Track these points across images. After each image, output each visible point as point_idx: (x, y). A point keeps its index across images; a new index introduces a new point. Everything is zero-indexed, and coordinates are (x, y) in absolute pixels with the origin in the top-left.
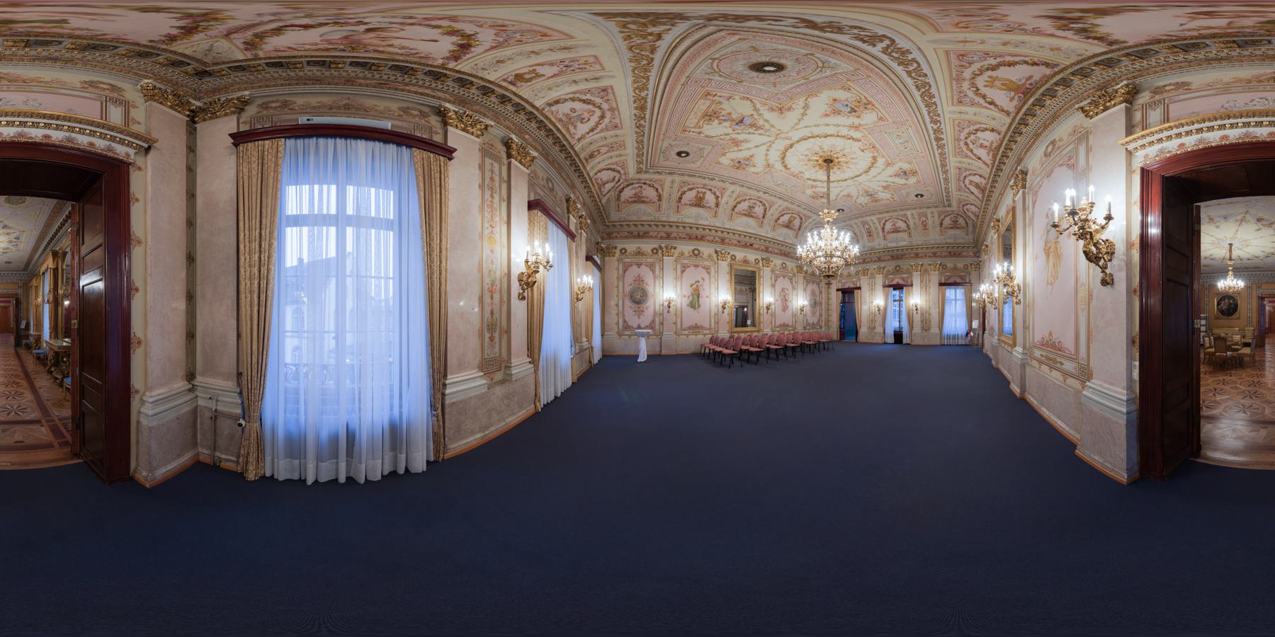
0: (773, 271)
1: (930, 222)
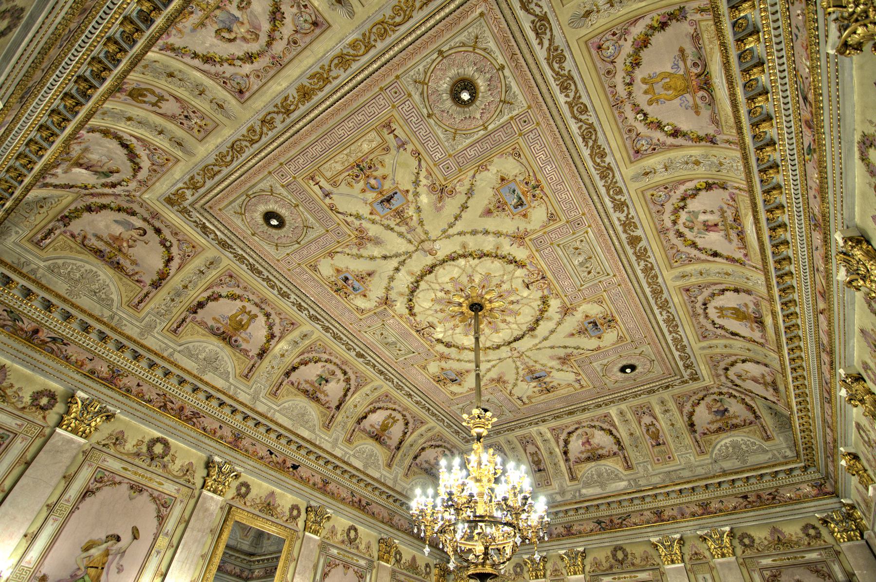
0: (324, 547)
1: (663, 424)
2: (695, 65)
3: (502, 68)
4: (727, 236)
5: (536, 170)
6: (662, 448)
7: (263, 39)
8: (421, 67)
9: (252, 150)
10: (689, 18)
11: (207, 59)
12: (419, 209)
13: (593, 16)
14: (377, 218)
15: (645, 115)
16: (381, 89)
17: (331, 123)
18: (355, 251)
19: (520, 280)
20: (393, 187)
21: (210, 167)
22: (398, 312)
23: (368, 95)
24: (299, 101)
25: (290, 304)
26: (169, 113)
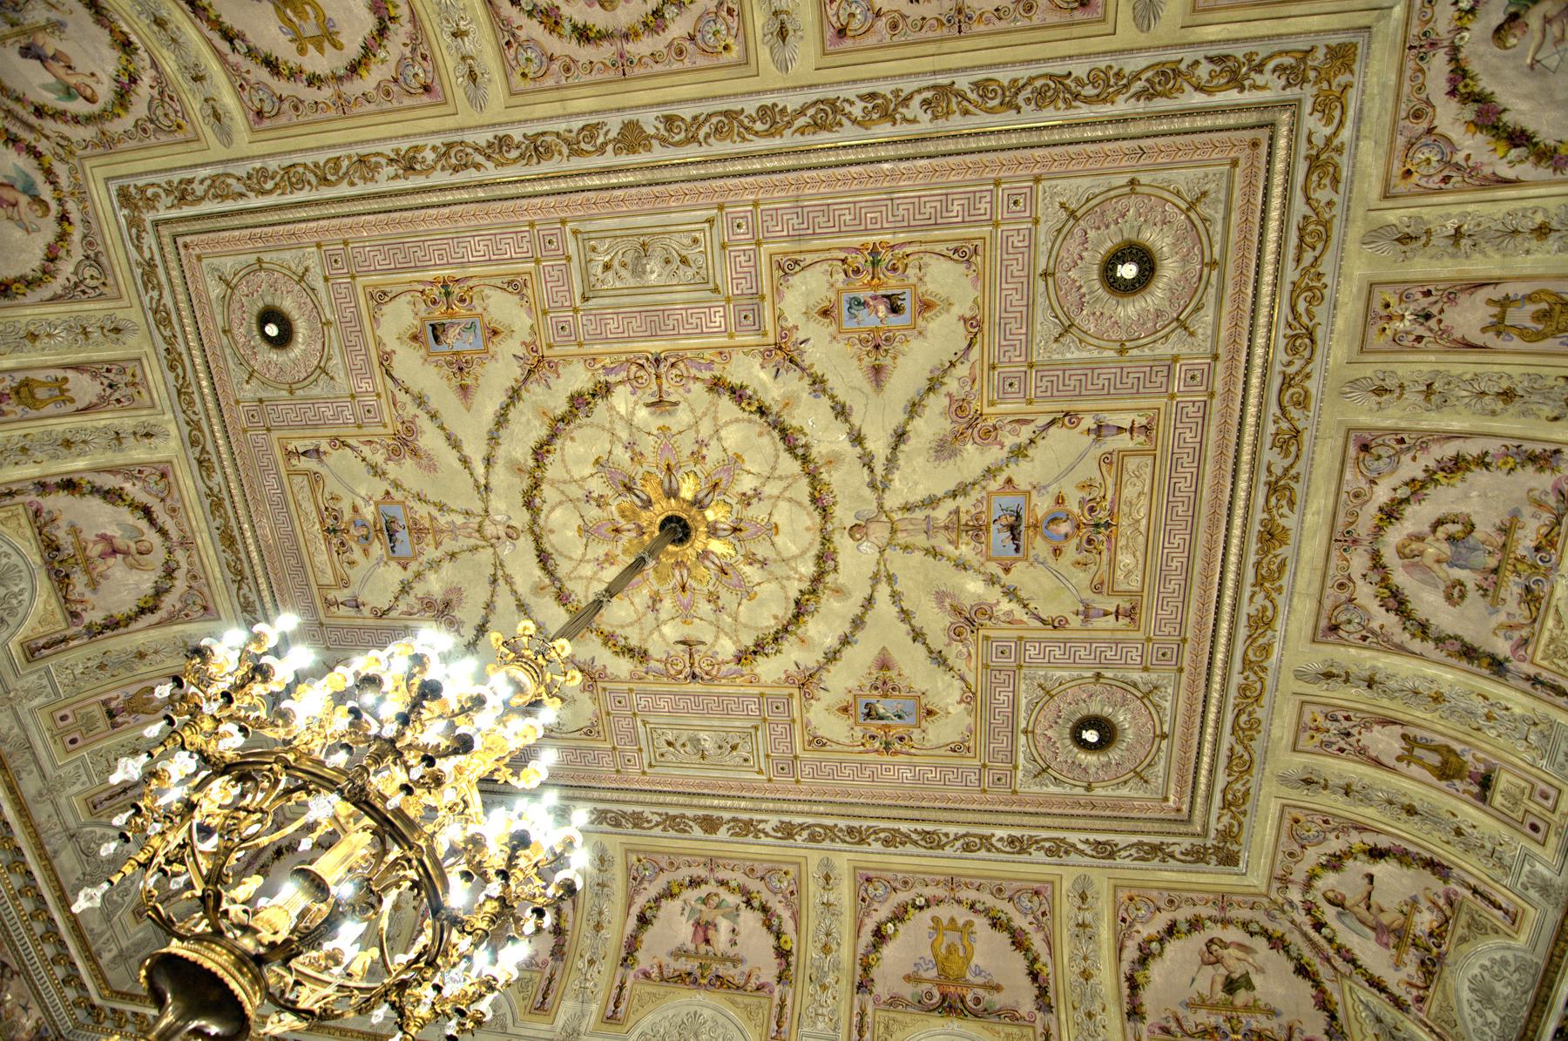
2: (977, 1001)
3: (1089, 788)
4: (680, 953)
5: (915, 759)
6: (103, 723)
7: (1389, 556)
8: (1167, 705)
9: (1278, 368)
10: (1039, 1015)
11: (1457, 465)
12: (962, 566)
13: (1078, 902)
14: (995, 485)
15: (921, 908)
16: (1184, 640)
17: (1202, 537)
18: (952, 385)
19: (708, 639)
20: (1032, 553)
21: (1319, 246)
22: (738, 356)
23: (1192, 617)
24: (1272, 519)
25: (908, 87)
26: (1464, 299)
